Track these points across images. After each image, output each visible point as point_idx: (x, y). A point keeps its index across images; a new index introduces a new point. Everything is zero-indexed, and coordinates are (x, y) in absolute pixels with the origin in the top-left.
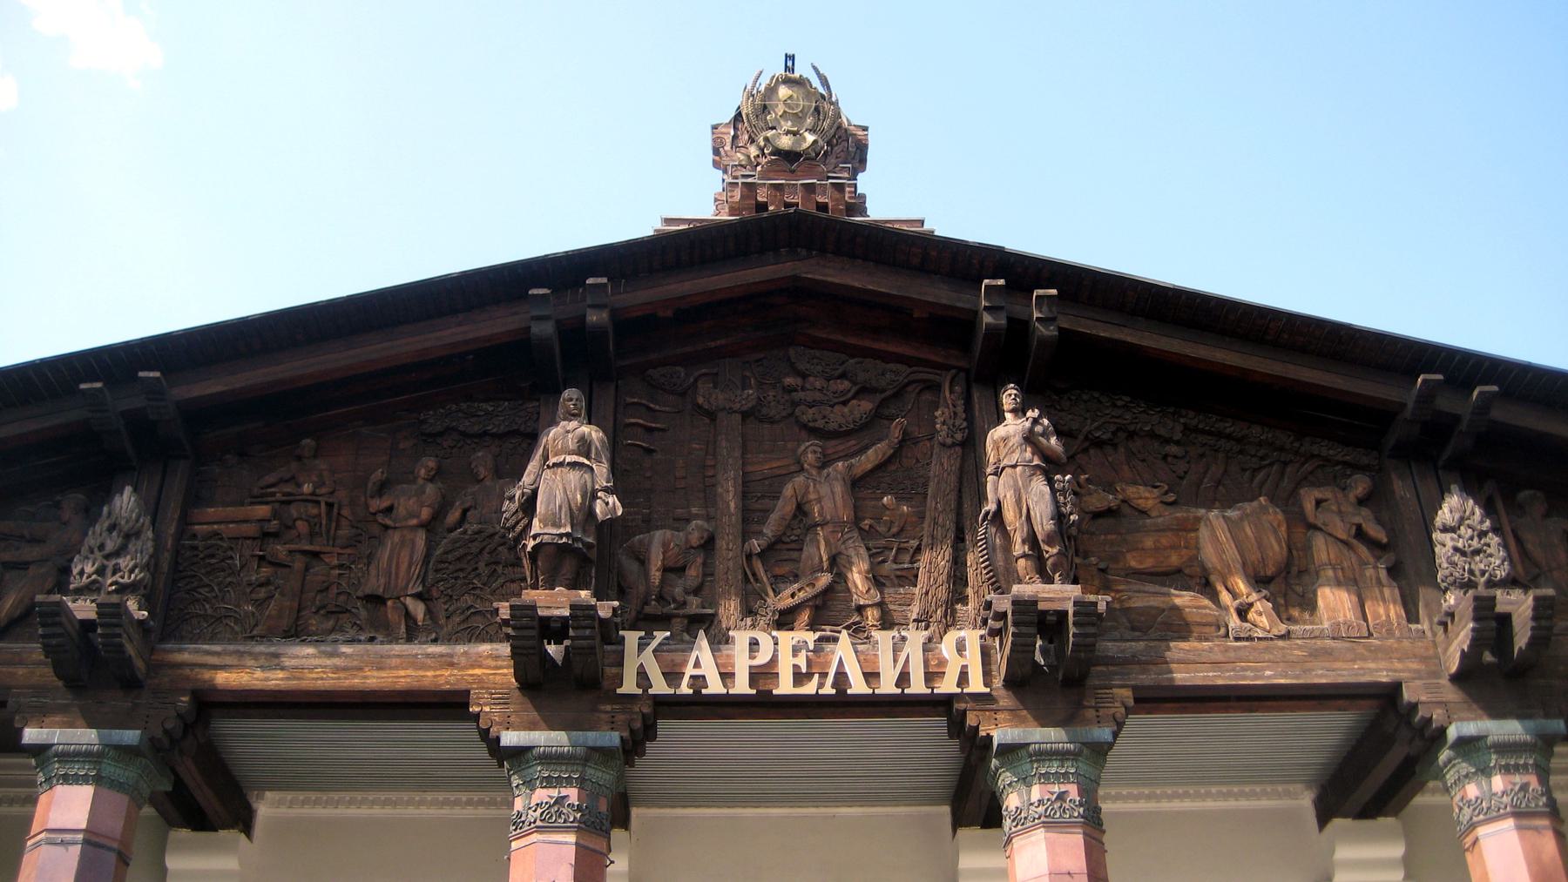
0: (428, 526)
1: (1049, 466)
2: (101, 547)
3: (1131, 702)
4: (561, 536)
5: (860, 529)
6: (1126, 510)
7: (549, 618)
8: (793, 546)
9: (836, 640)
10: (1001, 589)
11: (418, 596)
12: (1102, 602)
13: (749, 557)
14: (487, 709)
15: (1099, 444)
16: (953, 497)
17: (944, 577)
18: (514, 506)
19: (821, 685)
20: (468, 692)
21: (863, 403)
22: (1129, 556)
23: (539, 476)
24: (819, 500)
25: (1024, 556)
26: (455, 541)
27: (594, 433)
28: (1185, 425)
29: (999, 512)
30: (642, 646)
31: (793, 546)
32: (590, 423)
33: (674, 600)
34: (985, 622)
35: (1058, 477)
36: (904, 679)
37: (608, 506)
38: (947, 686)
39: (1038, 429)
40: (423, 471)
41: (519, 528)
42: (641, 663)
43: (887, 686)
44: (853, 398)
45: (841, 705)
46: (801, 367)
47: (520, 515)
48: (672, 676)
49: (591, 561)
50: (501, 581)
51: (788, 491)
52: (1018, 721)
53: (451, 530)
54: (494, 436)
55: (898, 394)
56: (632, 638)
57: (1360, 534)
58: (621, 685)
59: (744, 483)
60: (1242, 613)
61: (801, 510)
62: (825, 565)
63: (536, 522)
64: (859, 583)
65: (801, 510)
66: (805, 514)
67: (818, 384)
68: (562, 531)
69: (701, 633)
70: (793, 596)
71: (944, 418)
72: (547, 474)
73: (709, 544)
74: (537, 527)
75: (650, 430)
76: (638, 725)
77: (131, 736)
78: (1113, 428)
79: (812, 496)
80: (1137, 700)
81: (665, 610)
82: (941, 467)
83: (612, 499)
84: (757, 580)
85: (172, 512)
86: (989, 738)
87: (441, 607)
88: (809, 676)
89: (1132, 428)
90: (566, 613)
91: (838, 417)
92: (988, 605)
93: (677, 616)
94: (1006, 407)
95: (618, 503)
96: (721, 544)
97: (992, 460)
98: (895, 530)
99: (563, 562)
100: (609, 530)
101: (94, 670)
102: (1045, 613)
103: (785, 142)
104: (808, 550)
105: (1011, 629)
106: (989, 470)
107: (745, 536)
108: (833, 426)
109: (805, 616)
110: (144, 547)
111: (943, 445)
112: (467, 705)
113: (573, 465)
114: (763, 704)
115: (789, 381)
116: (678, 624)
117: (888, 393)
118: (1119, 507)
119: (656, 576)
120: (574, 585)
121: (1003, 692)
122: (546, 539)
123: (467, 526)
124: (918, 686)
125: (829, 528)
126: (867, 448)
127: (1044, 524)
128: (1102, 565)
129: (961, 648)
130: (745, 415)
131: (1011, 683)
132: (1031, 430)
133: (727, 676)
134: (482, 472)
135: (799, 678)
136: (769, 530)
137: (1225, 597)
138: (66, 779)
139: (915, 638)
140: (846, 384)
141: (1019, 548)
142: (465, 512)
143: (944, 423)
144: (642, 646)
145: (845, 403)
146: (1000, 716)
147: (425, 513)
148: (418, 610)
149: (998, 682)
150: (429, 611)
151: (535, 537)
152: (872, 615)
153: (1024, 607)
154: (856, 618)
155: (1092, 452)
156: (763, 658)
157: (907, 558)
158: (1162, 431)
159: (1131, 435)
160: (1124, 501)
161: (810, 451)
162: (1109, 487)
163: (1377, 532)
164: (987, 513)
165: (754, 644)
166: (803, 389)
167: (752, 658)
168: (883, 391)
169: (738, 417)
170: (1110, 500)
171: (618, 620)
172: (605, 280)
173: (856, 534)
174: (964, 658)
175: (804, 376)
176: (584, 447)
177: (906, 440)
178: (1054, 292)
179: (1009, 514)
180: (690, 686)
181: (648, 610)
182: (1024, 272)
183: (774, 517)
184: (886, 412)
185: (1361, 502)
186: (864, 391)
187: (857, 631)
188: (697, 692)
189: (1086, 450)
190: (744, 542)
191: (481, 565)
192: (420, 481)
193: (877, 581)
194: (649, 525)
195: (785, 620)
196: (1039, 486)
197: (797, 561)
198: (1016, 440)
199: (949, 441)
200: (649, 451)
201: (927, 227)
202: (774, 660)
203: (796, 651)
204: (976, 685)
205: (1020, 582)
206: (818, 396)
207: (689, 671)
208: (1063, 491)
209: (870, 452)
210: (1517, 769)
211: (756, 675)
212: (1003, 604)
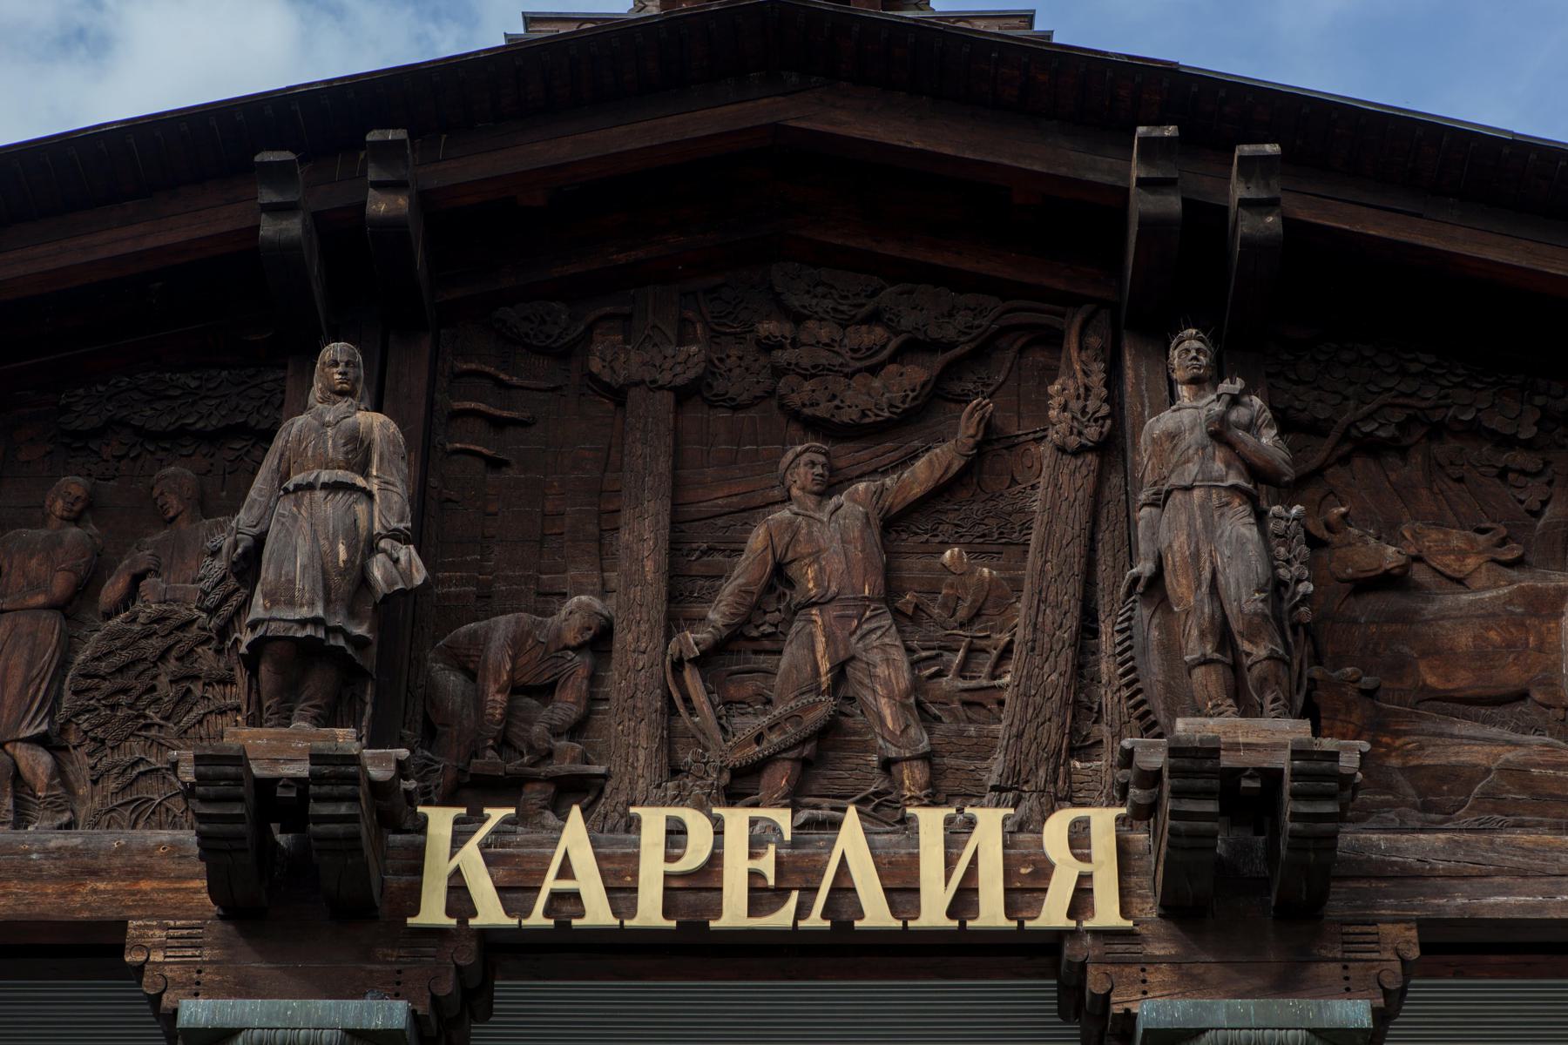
1: (1261, 487)
3: (1414, 953)
4: (303, 623)
5: (898, 614)
6: (1420, 574)
7: (274, 781)
8: (767, 644)
9: (836, 825)
10: (1149, 727)
11: (40, 741)
12: (1350, 755)
14: (157, 957)
15: (1372, 448)
16: (1076, 550)
17: (1055, 703)
18: (219, 566)
19: (802, 911)
20: (122, 925)
21: (908, 369)
22: (1423, 667)
23: (269, 511)
24: (816, 555)
25: (1205, 662)
26: (113, 636)
27: (376, 423)
28: (1542, 408)
29: (1157, 578)
30: (458, 841)
31: (767, 644)
32: (378, 408)
33: (531, 748)
34: (1124, 790)
35: (1276, 509)
36: (965, 899)
37: (399, 567)
38: (1053, 913)
39: (1239, 414)
40: (59, 504)
41: (226, 610)
42: (456, 864)
43: (933, 912)
44: (892, 359)
45: (843, 950)
46: (795, 302)
47: (232, 582)
48: (515, 893)
49: (364, 674)
50: (199, 711)
51: (757, 539)
52: (1189, 981)
53: (108, 616)
54: (202, 437)
55: (982, 353)
56: (441, 820)
58: (415, 911)
59: (675, 523)
61: (780, 576)
62: (825, 680)
63: (258, 600)
64: (887, 713)
65: (780, 576)
66: (790, 583)
67: (824, 334)
68: (305, 613)
69: (576, 811)
70: (759, 739)
71: (1068, 396)
72: (285, 506)
73: (600, 640)
74: (258, 609)
75: (498, 424)
76: (447, 987)
78: (1399, 416)
79: (802, 549)
80: (1426, 948)
81: (510, 767)
82: (1051, 489)
83: (406, 553)
84: (692, 711)
86: (1130, 1017)
87: (81, 762)
88: (781, 893)
89: (1437, 416)
90: (302, 769)
92: (1127, 757)
93: (534, 779)
94: (1178, 375)
95: (418, 561)
96: (624, 638)
97: (1149, 478)
98: (962, 613)
99: (306, 670)
100: (397, 610)
102: (1236, 773)
104: (792, 653)
105: (1168, 805)
106: (1143, 497)
107: (674, 622)
108: (849, 415)
109: (780, 777)
111: (1062, 449)
112: (120, 950)
113: (334, 487)
114: (691, 946)
115: (768, 328)
116: (534, 794)
117: (958, 351)
118: (1405, 568)
119: (496, 700)
120: (329, 718)
121: (1161, 928)
122: (275, 629)
123: (139, 605)
124: (991, 913)
125: (833, 611)
126: (915, 456)
127: (1245, 599)
128: (1368, 682)
129: (1079, 838)
130: (685, 395)
131: (1181, 909)
132: (1223, 419)
133: (622, 892)
134: (174, 505)
135: (761, 897)
136: (717, 615)
139: (990, 823)
140: (879, 333)
141: (1195, 646)
142: (137, 579)
143: (1065, 408)
144: (458, 841)
145: (874, 371)
146: (1154, 977)
147: (60, 584)
148: (37, 764)
149: (1149, 909)
150: (59, 771)
151: (254, 626)
152: (912, 777)
153: (1195, 761)
154: (879, 784)
155: (1358, 462)
156: (695, 856)
157: (986, 664)
158: (1496, 423)
159: (1437, 431)
160: (1418, 559)
161: (802, 463)
162: (1389, 531)
164: (1136, 580)
165: (676, 834)
166: (795, 343)
167: (669, 858)
168: (952, 345)
169: (669, 398)
170: (1391, 556)
171: (411, 785)
172: (401, 134)
173: (887, 621)
174: (1087, 864)
175: (798, 319)
176: (358, 452)
177: (991, 441)
178: (1271, 149)
179: (1179, 586)
180: (547, 913)
182: (1211, 112)
184: (957, 388)
186: (913, 347)
187: (886, 814)
188: (563, 926)
189: (1345, 460)
190: (668, 637)
191: (164, 680)
192: (54, 523)
193: (921, 708)
194: (486, 603)
195: (739, 787)
196: (1239, 525)
197: (770, 673)
198: (1199, 435)
199: (1073, 441)
200: (495, 464)
201: (1039, 26)
202: (715, 860)
203: (756, 847)
204: (1107, 912)
205: (1198, 712)
206: (823, 357)
207: (550, 883)
208: (1282, 537)
209: (920, 464)
211: (674, 890)
212: (1154, 757)
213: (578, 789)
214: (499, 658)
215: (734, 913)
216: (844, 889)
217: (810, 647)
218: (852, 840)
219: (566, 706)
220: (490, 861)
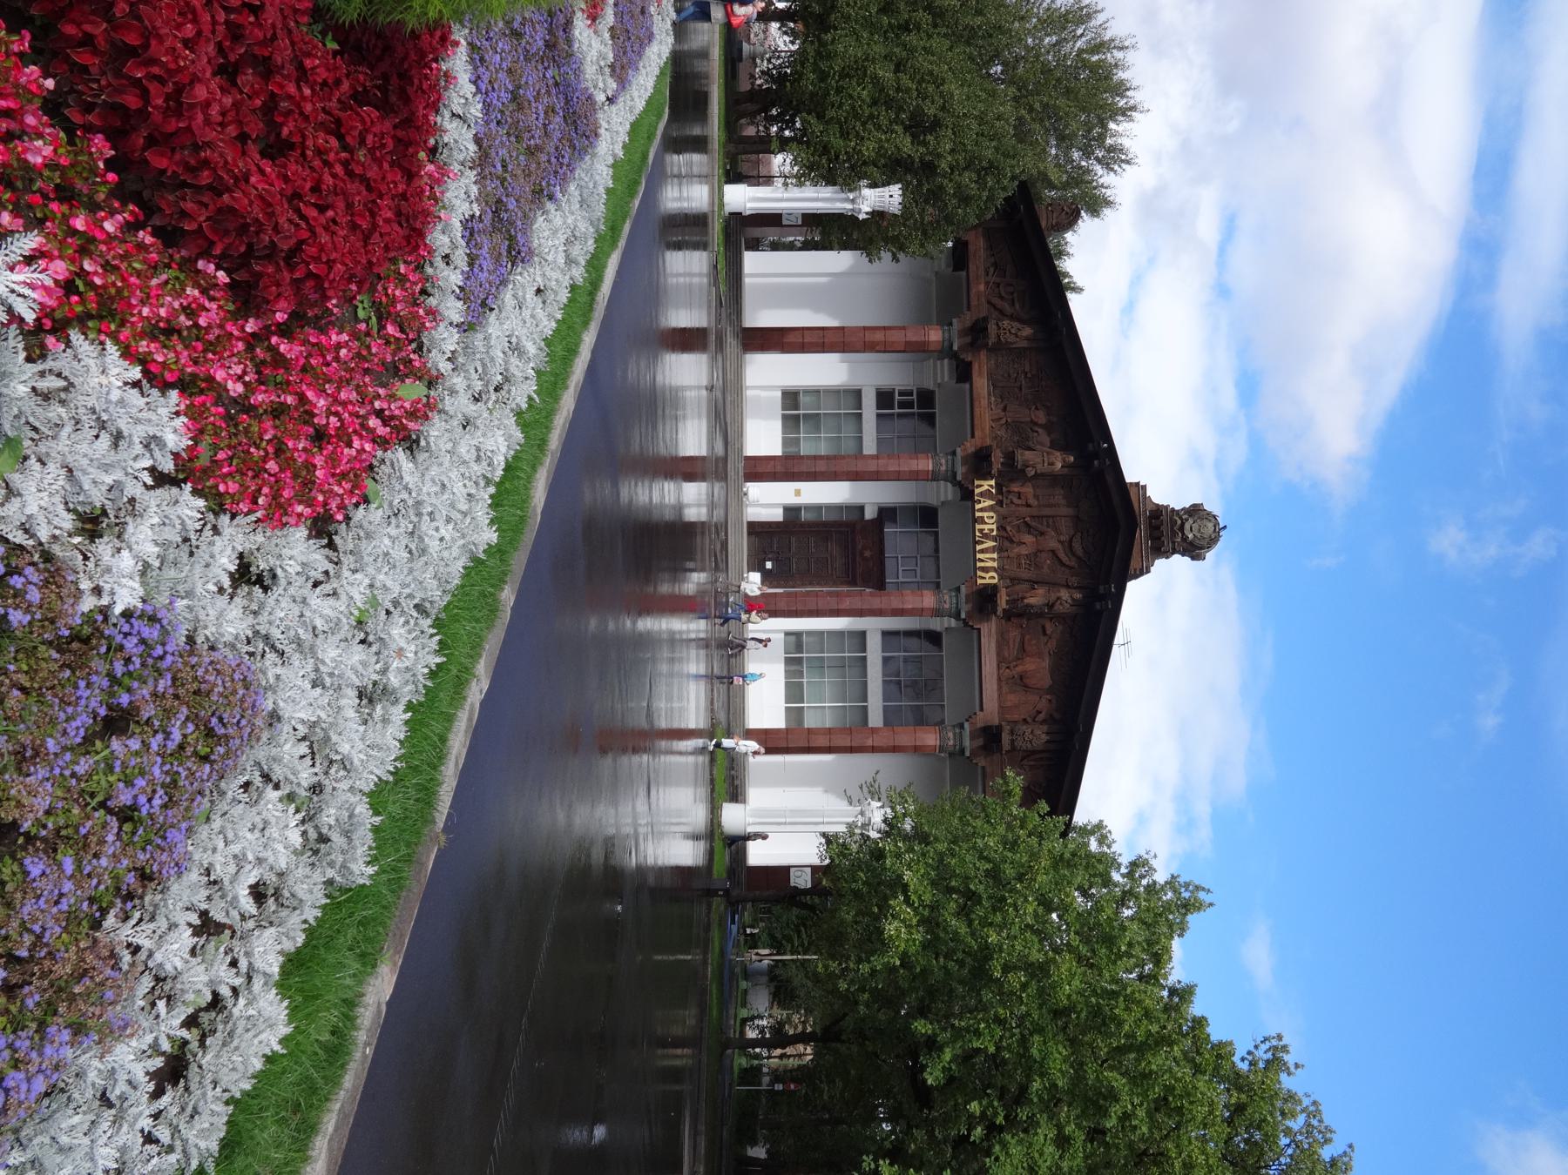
42: (987, 485)
43: (979, 556)
48: (981, 494)
56: (993, 482)
61: (1042, 534)
73: (1028, 506)
77: (955, 348)
85: (1024, 344)
91: (1077, 546)
101: (977, 332)
103: (1187, 526)
110: (1011, 339)
133: (981, 510)
135: (981, 531)
193: (1019, 556)
204: (980, 581)
213: (1000, 503)
214: (1023, 490)
215: (978, 527)
217: (1028, 539)
219: (1016, 500)
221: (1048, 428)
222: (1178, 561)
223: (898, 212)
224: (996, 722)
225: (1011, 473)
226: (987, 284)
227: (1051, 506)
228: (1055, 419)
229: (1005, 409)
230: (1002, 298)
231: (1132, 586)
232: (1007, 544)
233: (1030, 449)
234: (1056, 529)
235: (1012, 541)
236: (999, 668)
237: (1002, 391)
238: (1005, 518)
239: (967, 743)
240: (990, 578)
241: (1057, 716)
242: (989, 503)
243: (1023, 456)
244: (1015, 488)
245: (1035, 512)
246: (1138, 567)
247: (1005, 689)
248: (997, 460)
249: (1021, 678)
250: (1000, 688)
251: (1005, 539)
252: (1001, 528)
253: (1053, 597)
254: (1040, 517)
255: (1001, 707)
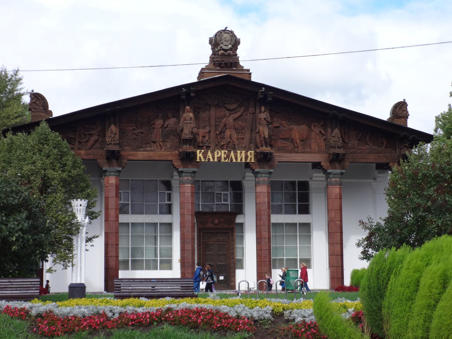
0: (161, 127)
2: (111, 136)
13: (216, 134)
29: (259, 132)
30: (200, 153)
38: (248, 161)
42: (199, 155)
48: (205, 158)
51: (223, 121)
56: (198, 151)
57: (320, 132)
60: (297, 147)
61: (225, 125)
68: (188, 136)
73: (210, 132)
83: (196, 129)
96: (211, 132)
98: (241, 128)
103: (225, 48)
108: (231, 109)
119: (201, 138)
133: (213, 158)
135: (225, 159)
136: (220, 130)
137: (295, 144)
138: (111, 175)
139: (244, 152)
142: (168, 125)
144: (200, 153)
147: (161, 125)
148: (162, 144)
156: (219, 156)
163: (323, 131)
181: (200, 145)
183: (221, 126)
185: (322, 126)
202: (221, 156)
204: (253, 161)
207: (208, 157)
210: (336, 177)
211: (218, 158)
215: (223, 160)
216: (232, 158)
217: (228, 133)
218: (232, 154)
219: (207, 139)
220: (203, 155)
221: (165, 118)
222: (241, 52)
223: (87, 201)
224: (327, 155)
225: (193, 141)
226: (79, 149)
227: (209, 119)
228: (160, 115)
229: (155, 142)
230: (88, 141)
231: (254, 78)
232: (230, 145)
233: (182, 130)
234: (222, 118)
235: (229, 142)
236: (298, 152)
237: (145, 143)
238: (216, 145)
239: (338, 171)
240: (251, 154)
241: (322, 123)
242: (209, 154)
243: (187, 134)
244: (200, 139)
245: (213, 129)
246: (248, 75)
247: (308, 150)
248: (187, 148)
249: (302, 141)
250: (308, 152)
251: (231, 146)
252: (222, 148)
253: (264, 122)
254: (216, 126)
255: (318, 153)
